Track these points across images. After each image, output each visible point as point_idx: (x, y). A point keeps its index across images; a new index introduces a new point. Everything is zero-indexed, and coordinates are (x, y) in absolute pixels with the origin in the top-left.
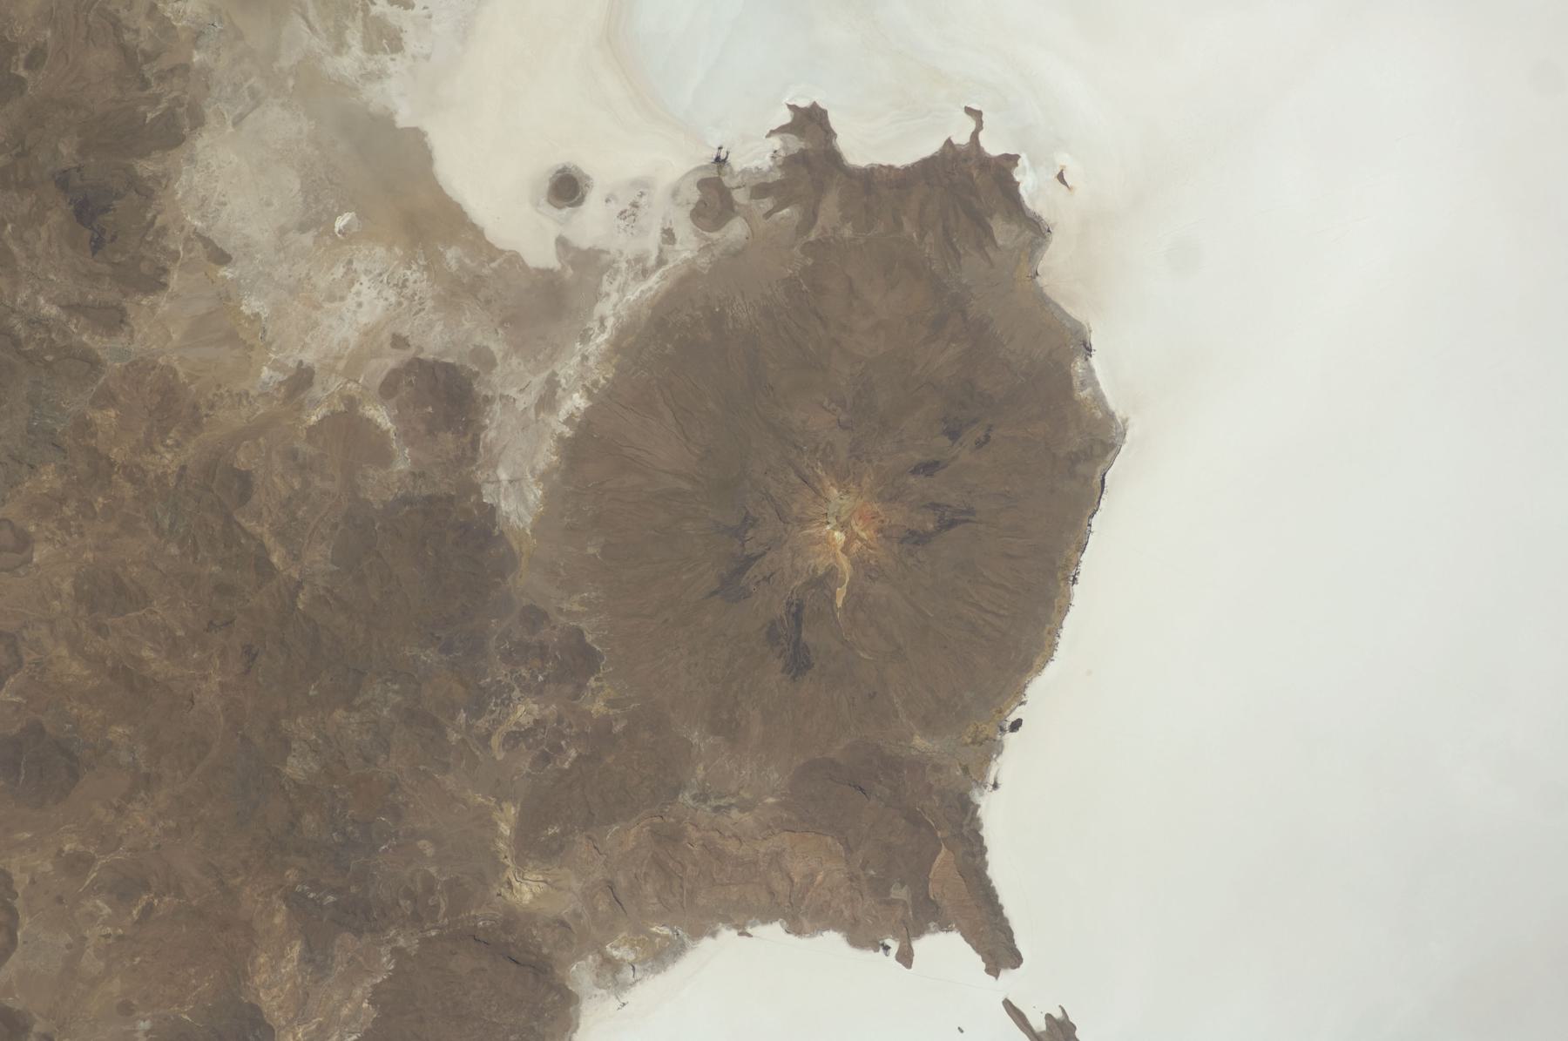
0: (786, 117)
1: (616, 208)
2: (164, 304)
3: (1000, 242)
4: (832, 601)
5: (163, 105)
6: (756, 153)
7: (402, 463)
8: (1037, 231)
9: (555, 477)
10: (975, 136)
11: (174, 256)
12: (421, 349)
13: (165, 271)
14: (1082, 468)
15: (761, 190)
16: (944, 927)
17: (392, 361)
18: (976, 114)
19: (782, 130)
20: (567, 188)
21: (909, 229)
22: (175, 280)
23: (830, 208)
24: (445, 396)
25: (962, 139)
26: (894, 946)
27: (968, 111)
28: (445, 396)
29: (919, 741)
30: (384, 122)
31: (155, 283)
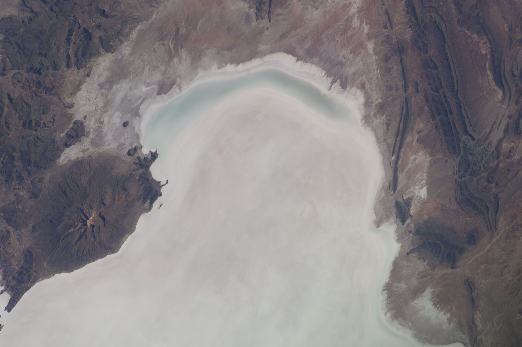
0: (153, 151)
3: (145, 205)
4: (70, 229)
5: (114, 44)
6: (145, 151)
11: (86, 67)
12: (85, 122)
13: (82, 67)
15: (138, 158)
18: (167, 182)
19: (151, 152)
22: (82, 70)
24: (77, 133)
25: (162, 184)
27: (167, 181)
28: (77, 133)
29: (45, 263)
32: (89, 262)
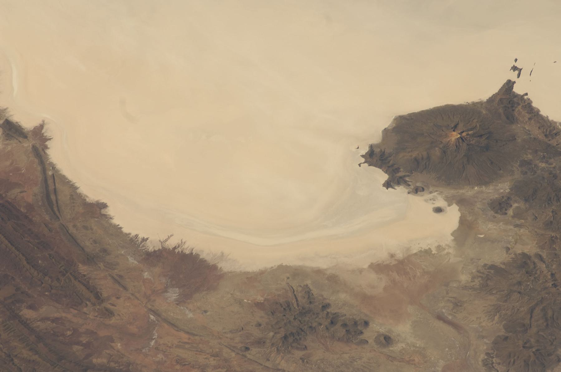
0: (390, 189)
1: (434, 202)
2: (526, 251)
7: (515, 205)
8: (371, 147)
9: (494, 184)
10: (364, 163)
14: (408, 118)
16: (514, 92)
17: (499, 216)
18: (360, 165)
20: (438, 210)
21: (391, 162)
22: (520, 252)
23: (400, 174)
25: (366, 165)
26: (526, 97)
29: (484, 112)
30: (455, 240)
31: (524, 255)
32: (427, 111)
